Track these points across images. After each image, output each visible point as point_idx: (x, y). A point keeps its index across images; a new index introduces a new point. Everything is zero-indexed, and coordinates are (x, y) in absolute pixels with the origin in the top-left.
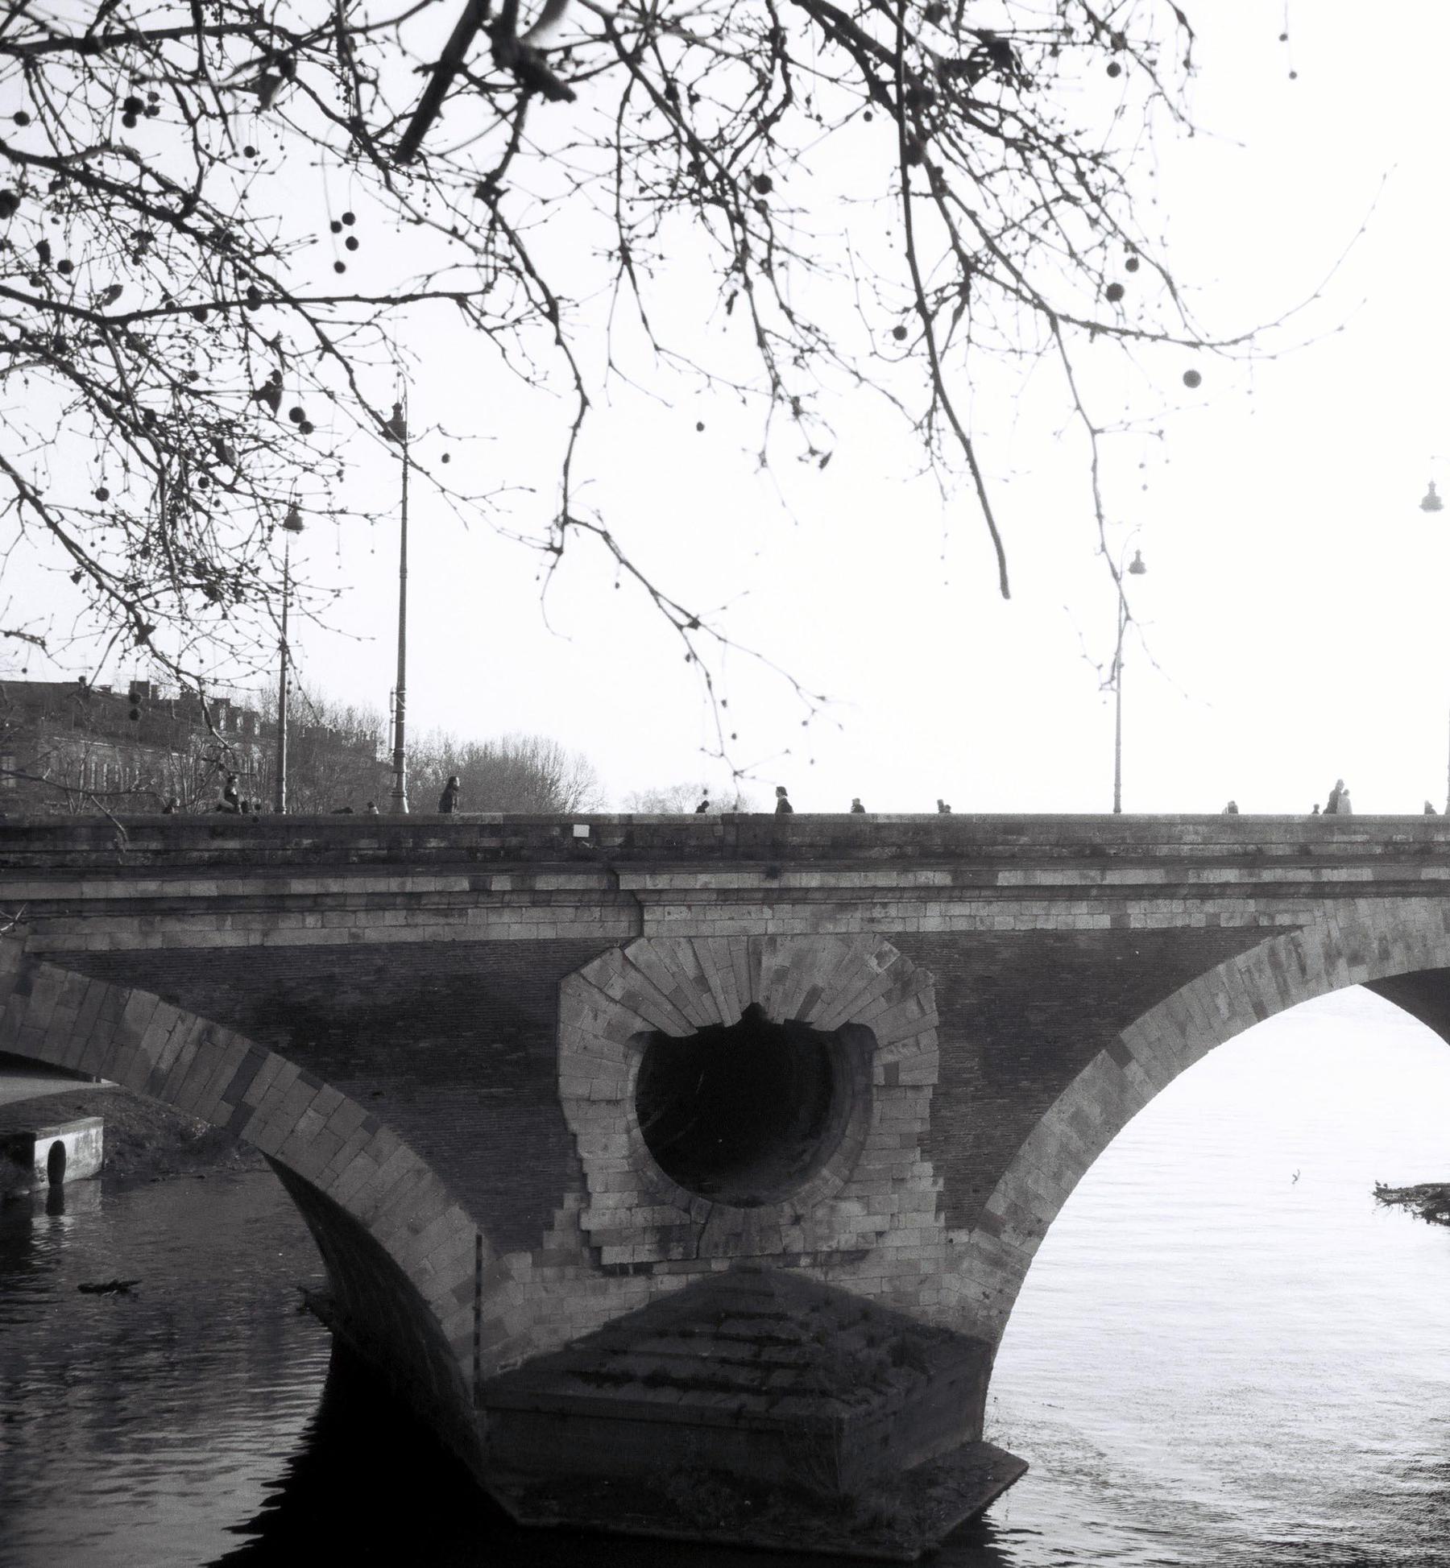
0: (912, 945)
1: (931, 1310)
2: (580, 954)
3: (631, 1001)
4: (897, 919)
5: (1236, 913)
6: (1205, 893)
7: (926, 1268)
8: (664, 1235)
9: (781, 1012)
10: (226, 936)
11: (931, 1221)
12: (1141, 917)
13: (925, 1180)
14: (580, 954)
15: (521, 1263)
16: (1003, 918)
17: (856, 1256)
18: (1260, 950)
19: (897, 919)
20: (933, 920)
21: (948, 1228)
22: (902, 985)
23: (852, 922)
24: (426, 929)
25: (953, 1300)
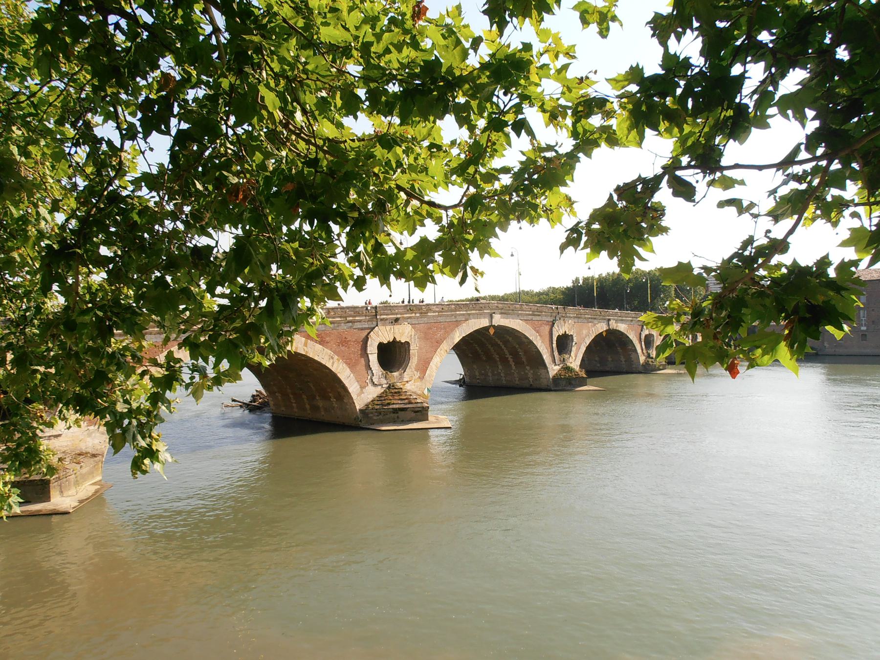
1: (84, 448)
7: (81, 437)
21: (88, 426)
25: (90, 444)
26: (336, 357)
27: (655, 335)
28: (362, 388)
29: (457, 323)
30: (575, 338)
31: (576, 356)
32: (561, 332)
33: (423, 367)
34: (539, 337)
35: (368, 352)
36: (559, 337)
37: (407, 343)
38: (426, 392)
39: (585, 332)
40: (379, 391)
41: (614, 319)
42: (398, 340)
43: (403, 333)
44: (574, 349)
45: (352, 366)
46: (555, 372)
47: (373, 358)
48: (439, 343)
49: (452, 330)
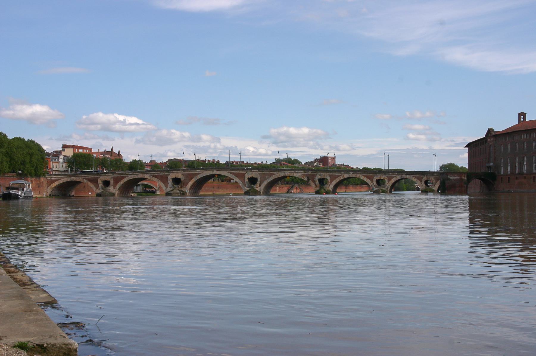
0: (112, 177)
2: (98, 178)
3: (101, 180)
4: (111, 176)
5: (126, 176)
6: (124, 175)
8: (102, 189)
9: (106, 180)
10: (87, 177)
11: (113, 189)
12: (122, 176)
13: (113, 187)
14: (98, 178)
15: (97, 190)
16: (115, 176)
17: (110, 190)
18: (127, 177)
19: (111, 176)
20: (113, 176)
22: (111, 179)
23: (109, 176)
24: (94, 177)
26: (160, 181)
27: (329, 178)
28: (167, 187)
29: (199, 174)
30: (259, 179)
31: (260, 186)
32: (250, 176)
33: (186, 184)
34: (237, 178)
35: (168, 180)
36: (249, 179)
37: (180, 179)
38: (186, 191)
39: (267, 177)
40: (171, 189)
41: (288, 172)
42: (177, 177)
43: (180, 175)
44: (258, 183)
45: (164, 183)
46: (247, 190)
47: (170, 182)
48: (192, 178)
49: (197, 175)
